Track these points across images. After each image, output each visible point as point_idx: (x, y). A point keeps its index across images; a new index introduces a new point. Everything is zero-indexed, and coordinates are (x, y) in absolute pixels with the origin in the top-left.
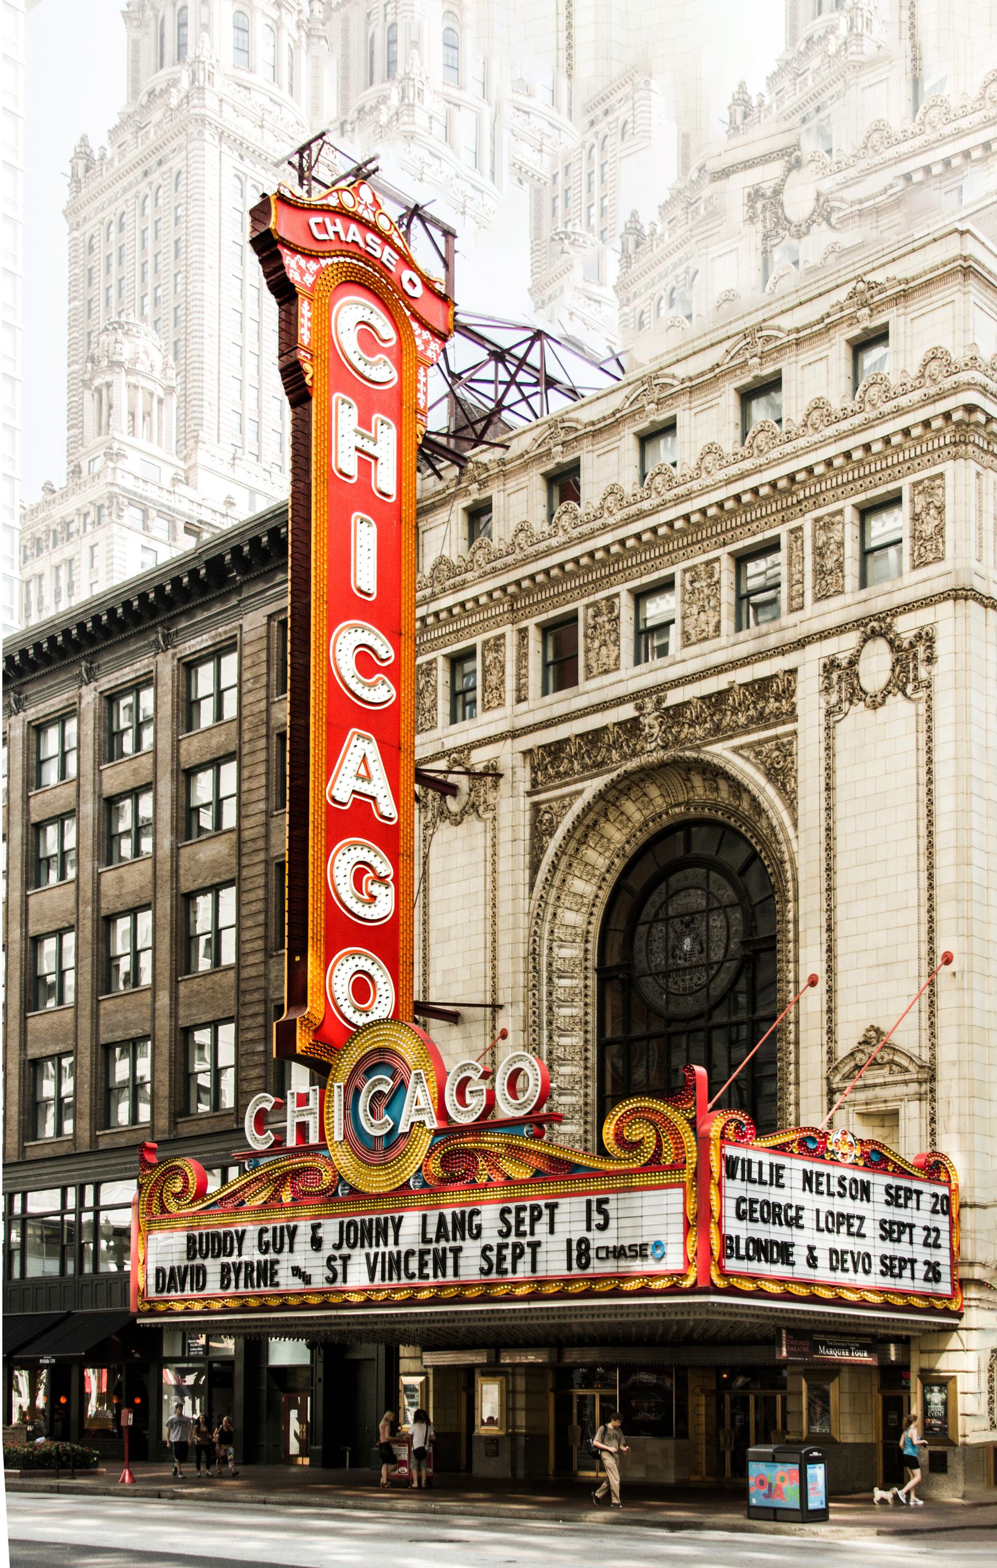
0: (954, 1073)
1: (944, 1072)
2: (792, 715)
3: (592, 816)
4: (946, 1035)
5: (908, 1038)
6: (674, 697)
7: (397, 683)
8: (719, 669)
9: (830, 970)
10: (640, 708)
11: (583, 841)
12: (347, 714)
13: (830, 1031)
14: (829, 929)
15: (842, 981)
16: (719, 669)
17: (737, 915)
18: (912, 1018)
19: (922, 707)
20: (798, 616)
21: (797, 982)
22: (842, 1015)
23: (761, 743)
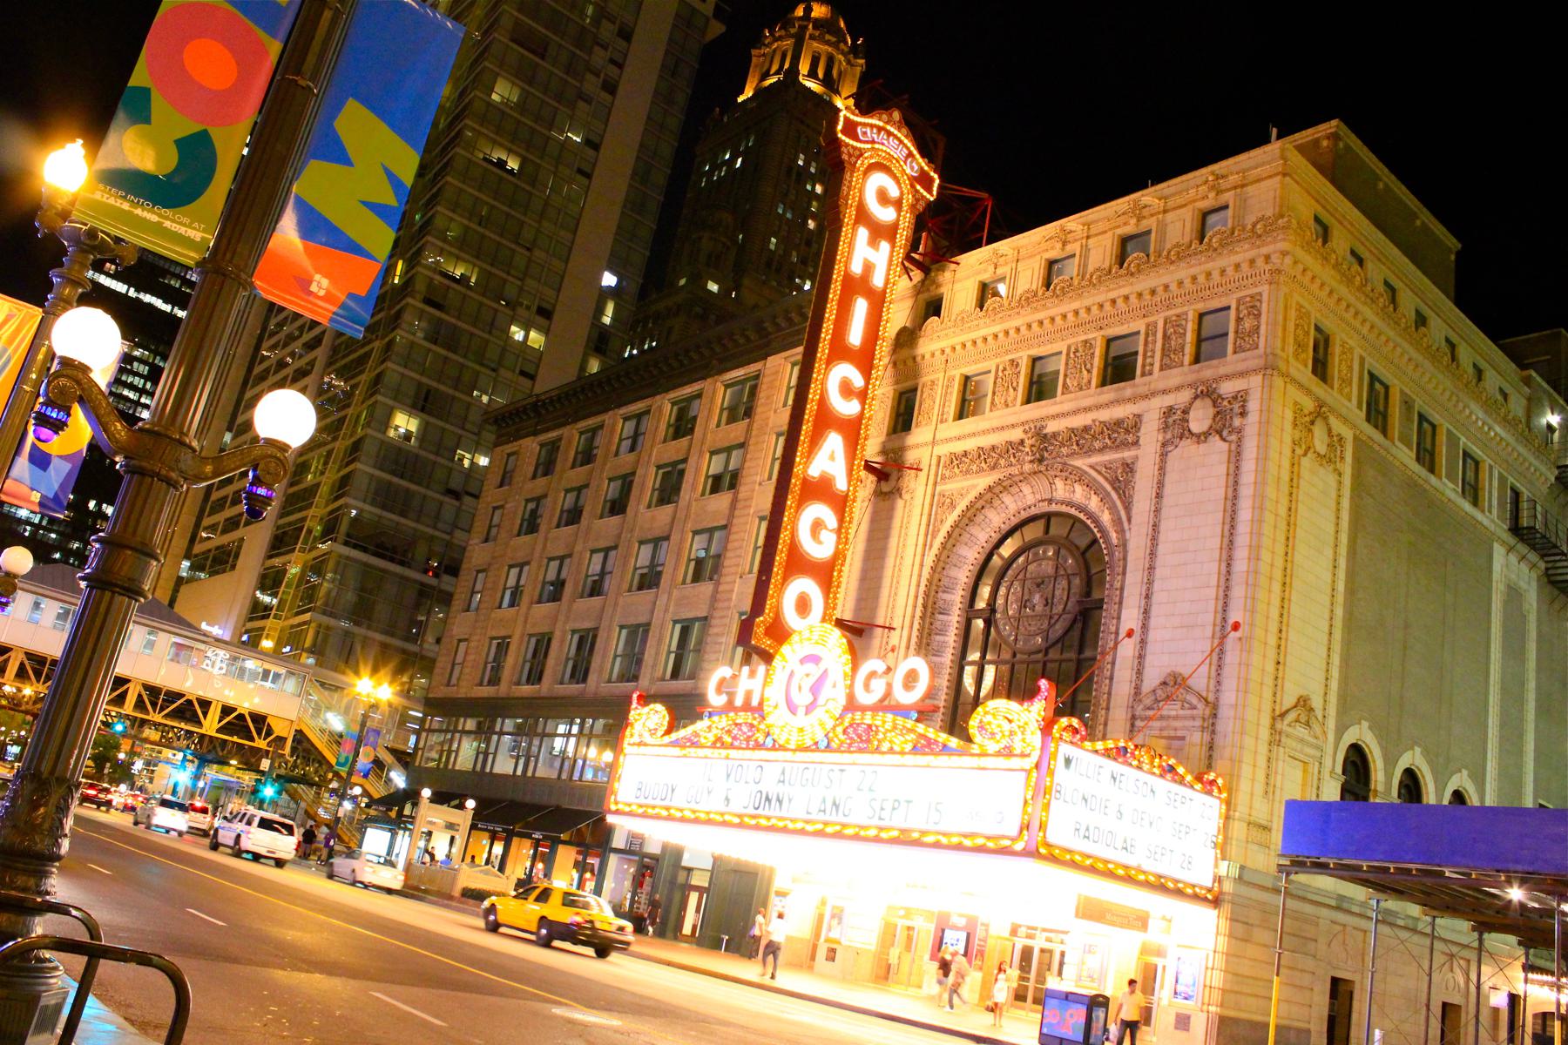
0: (1232, 713)
1: (1225, 712)
2: (1136, 443)
3: (981, 503)
4: (1229, 684)
5: (1200, 682)
6: (1051, 427)
7: (863, 403)
8: (1087, 409)
9: (1145, 627)
10: (1025, 432)
11: (971, 520)
12: (827, 420)
13: (1139, 673)
14: (1147, 597)
15: (1152, 636)
16: (1087, 409)
17: (1077, 581)
18: (1204, 669)
19: (1233, 447)
20: (1147, 379)
21: (1117, 633)
22: (1149, 660)
23: (1110, 462)
